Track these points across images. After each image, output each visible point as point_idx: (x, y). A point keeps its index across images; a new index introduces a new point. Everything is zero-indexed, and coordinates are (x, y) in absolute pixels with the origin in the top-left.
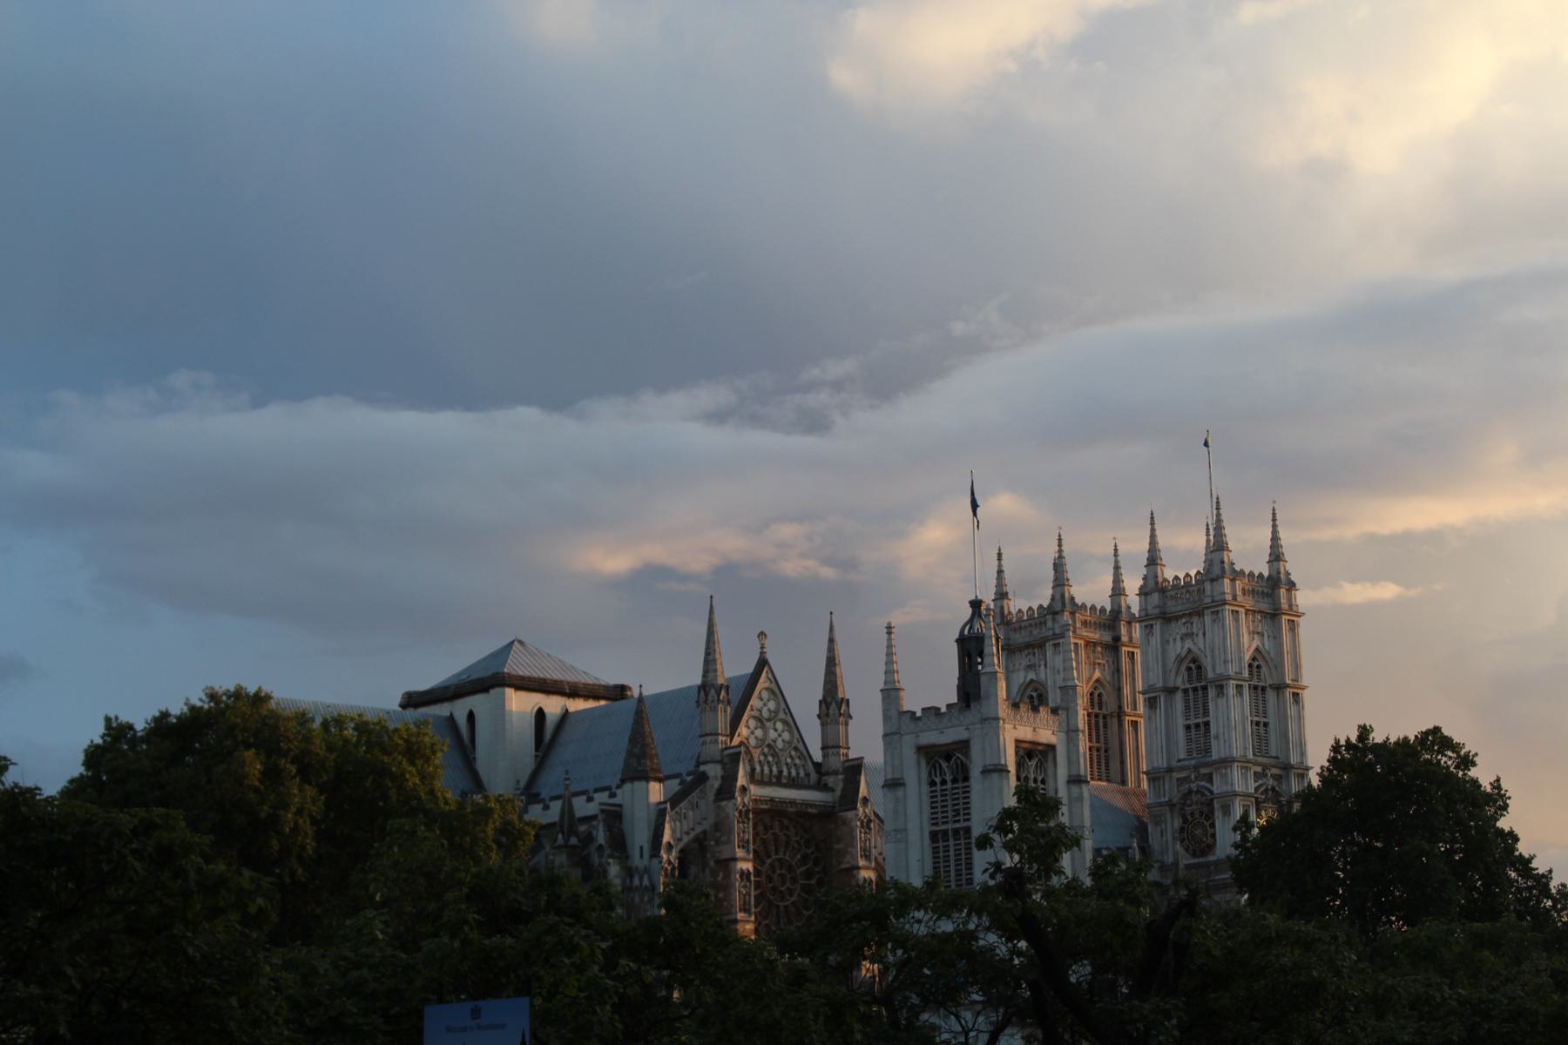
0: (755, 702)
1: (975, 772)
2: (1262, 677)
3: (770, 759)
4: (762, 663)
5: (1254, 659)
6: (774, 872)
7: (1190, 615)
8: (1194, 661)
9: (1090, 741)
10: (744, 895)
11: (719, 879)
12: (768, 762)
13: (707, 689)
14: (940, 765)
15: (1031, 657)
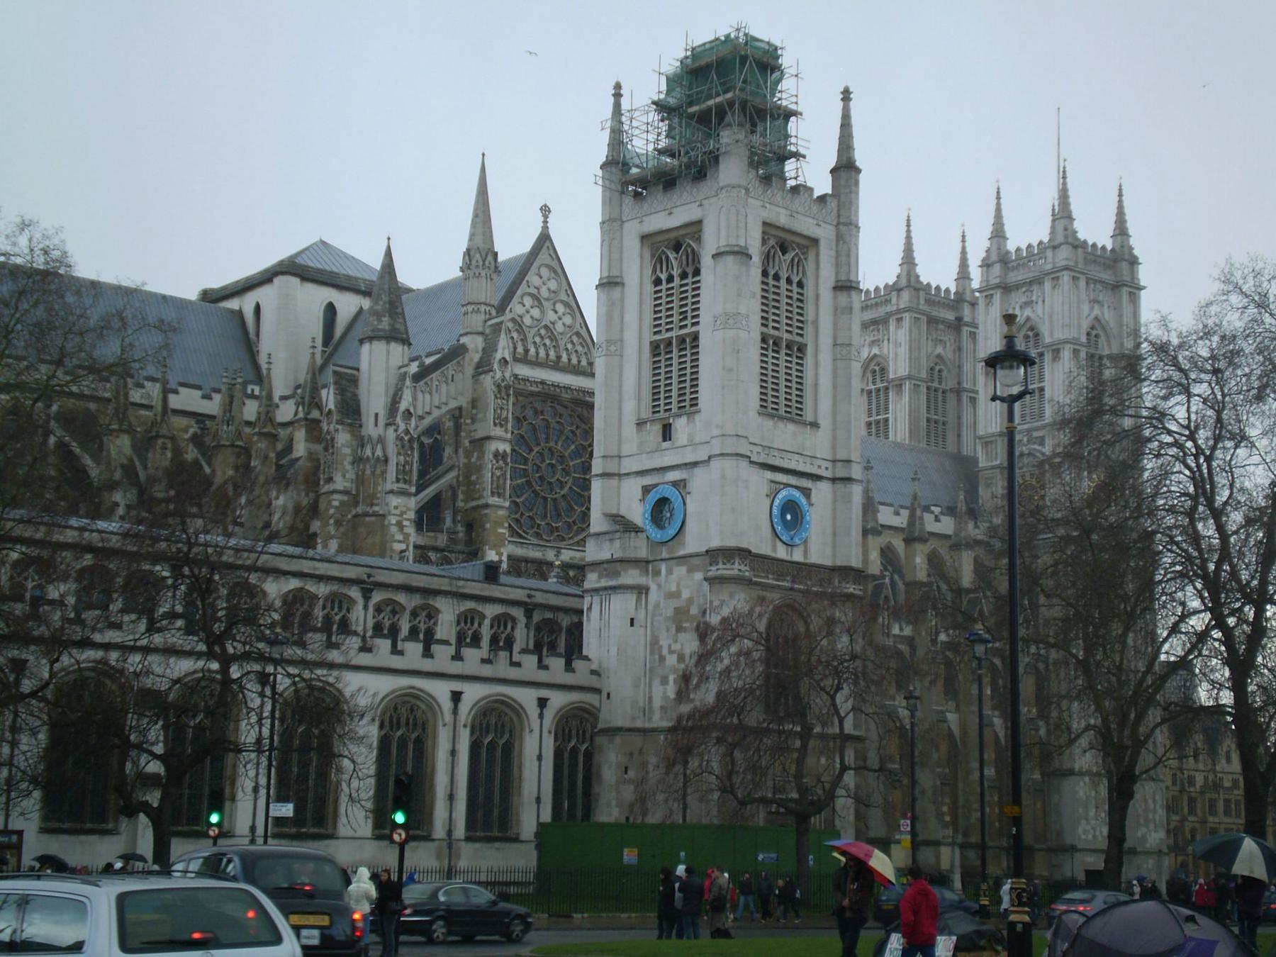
0: (532, 278)
1: (706, 261)
2: (1100, 346)
3: (548, 342)
4: (544, 239)
5: (1093, 328)
6: (543, 461)
7: (1031, 283)
8: (1032, 329)
9: (928, 411)
10: (498, 478)
11: (473, 460)
12: (545, 345)
13: (472, 253)
14: (667, 258)
15: (876, 333)
